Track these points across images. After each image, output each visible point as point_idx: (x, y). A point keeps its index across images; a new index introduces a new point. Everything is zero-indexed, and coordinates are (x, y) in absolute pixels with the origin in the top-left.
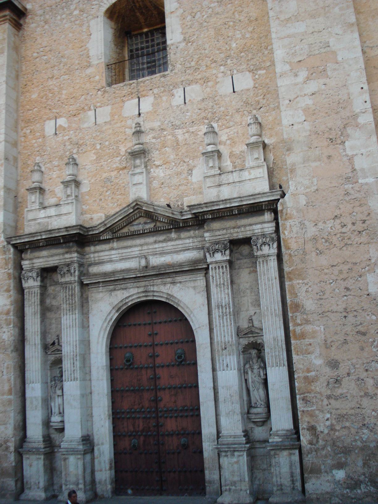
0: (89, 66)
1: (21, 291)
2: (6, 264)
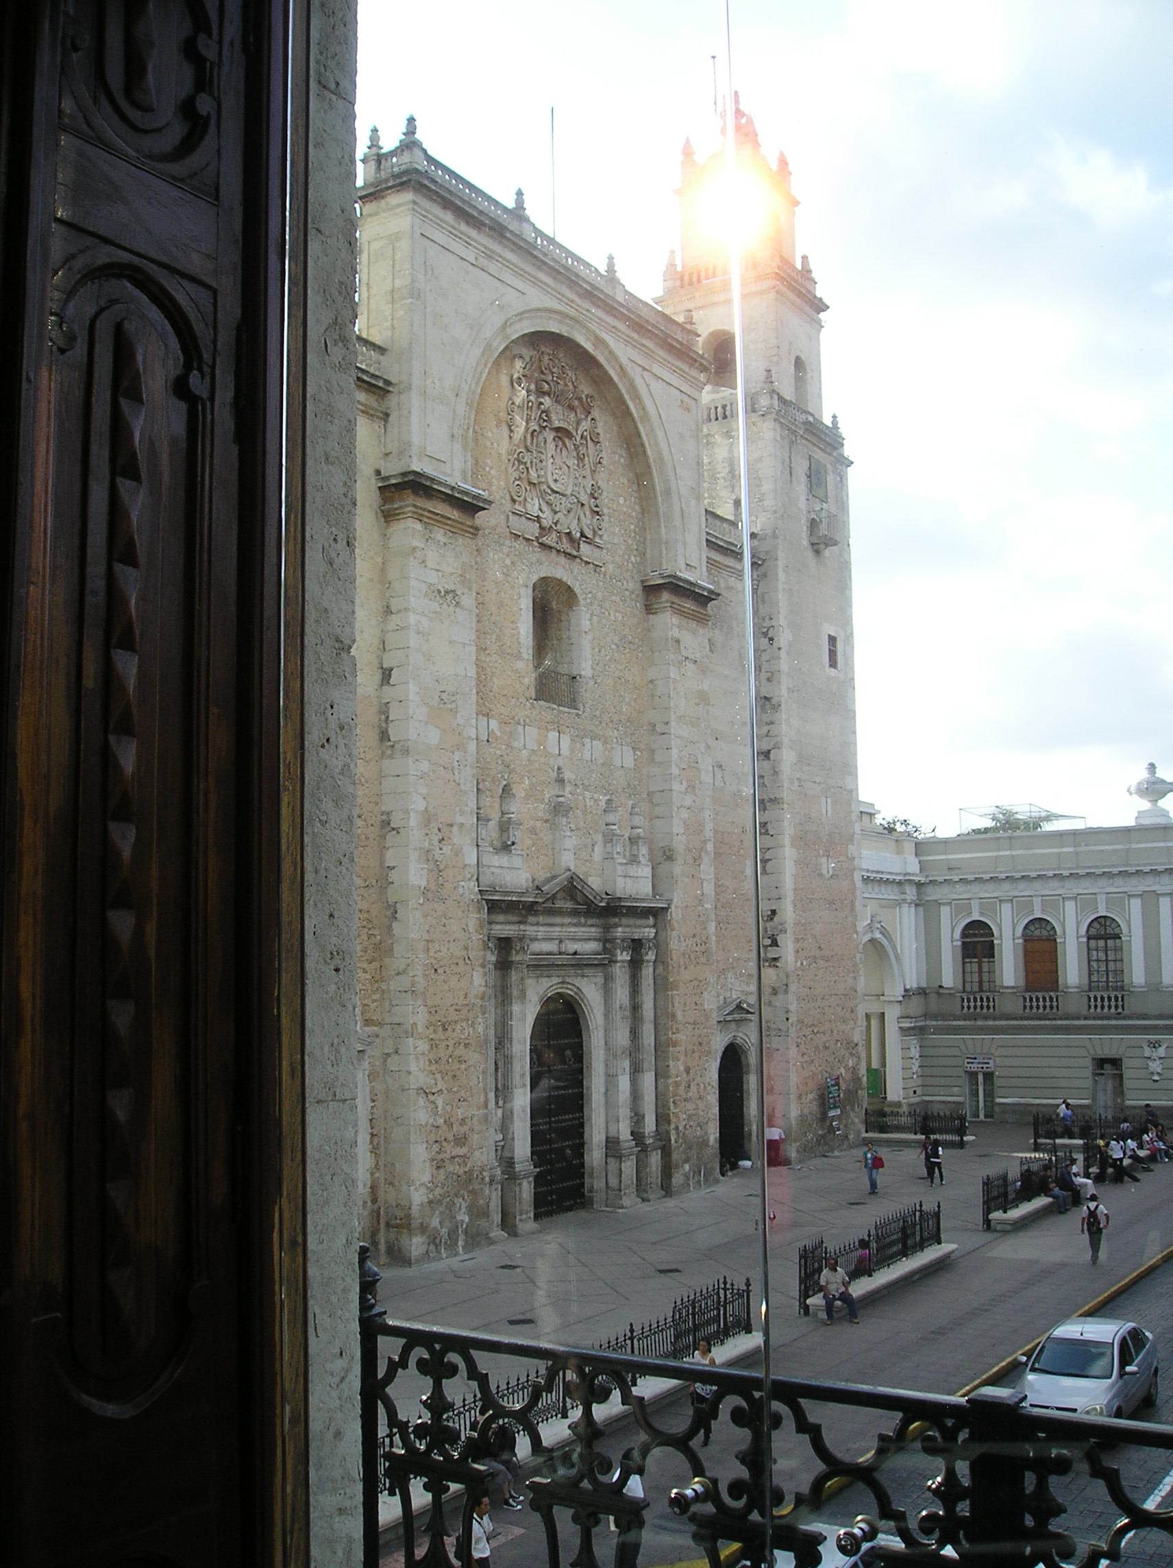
0: (519, 657)
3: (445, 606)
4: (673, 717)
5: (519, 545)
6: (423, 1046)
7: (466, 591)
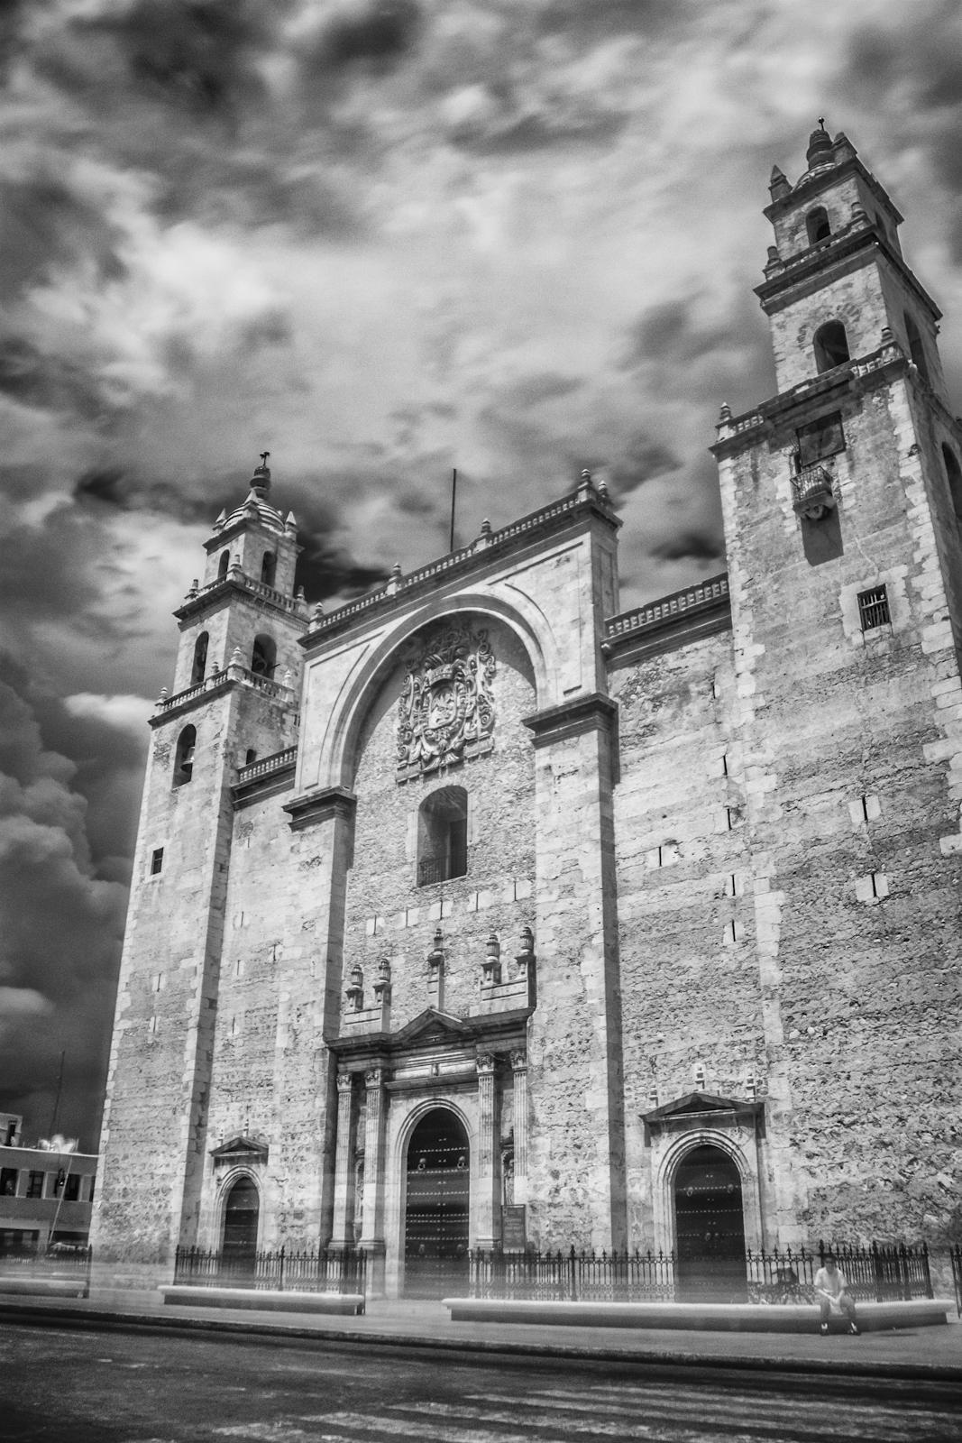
1: (334, 1094)
2: (323, 1067)
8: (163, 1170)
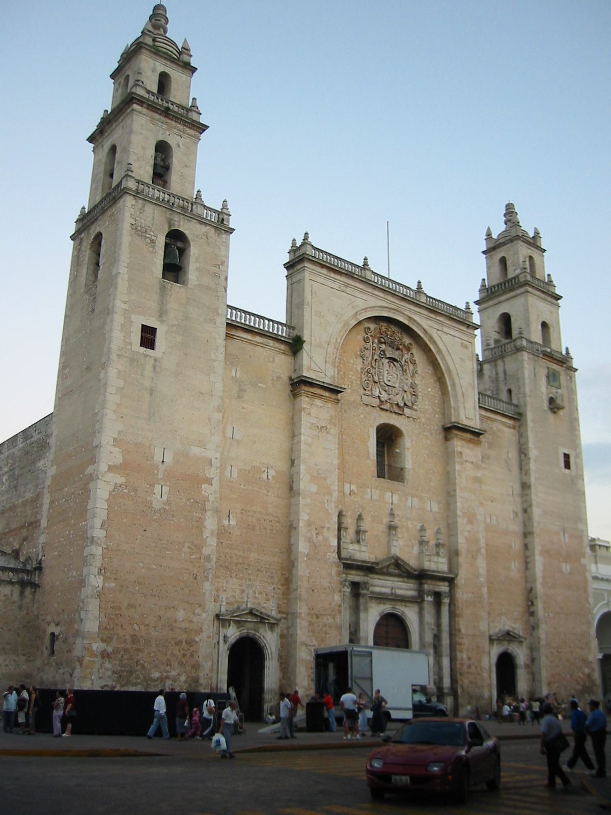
3: (321, 433)
4: (457, 488)
5: (368, 409)
6: (305, 624)
7: (332, 427)
8: (185, 625)
